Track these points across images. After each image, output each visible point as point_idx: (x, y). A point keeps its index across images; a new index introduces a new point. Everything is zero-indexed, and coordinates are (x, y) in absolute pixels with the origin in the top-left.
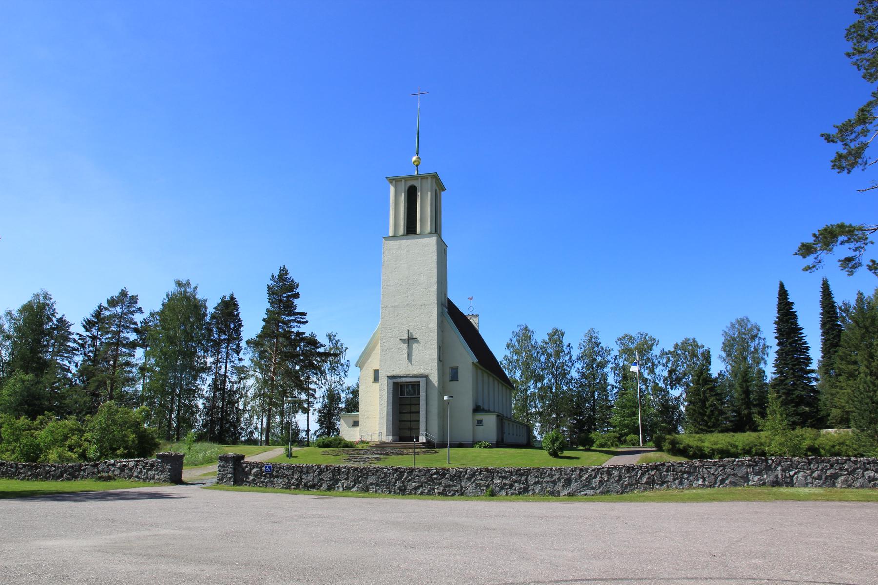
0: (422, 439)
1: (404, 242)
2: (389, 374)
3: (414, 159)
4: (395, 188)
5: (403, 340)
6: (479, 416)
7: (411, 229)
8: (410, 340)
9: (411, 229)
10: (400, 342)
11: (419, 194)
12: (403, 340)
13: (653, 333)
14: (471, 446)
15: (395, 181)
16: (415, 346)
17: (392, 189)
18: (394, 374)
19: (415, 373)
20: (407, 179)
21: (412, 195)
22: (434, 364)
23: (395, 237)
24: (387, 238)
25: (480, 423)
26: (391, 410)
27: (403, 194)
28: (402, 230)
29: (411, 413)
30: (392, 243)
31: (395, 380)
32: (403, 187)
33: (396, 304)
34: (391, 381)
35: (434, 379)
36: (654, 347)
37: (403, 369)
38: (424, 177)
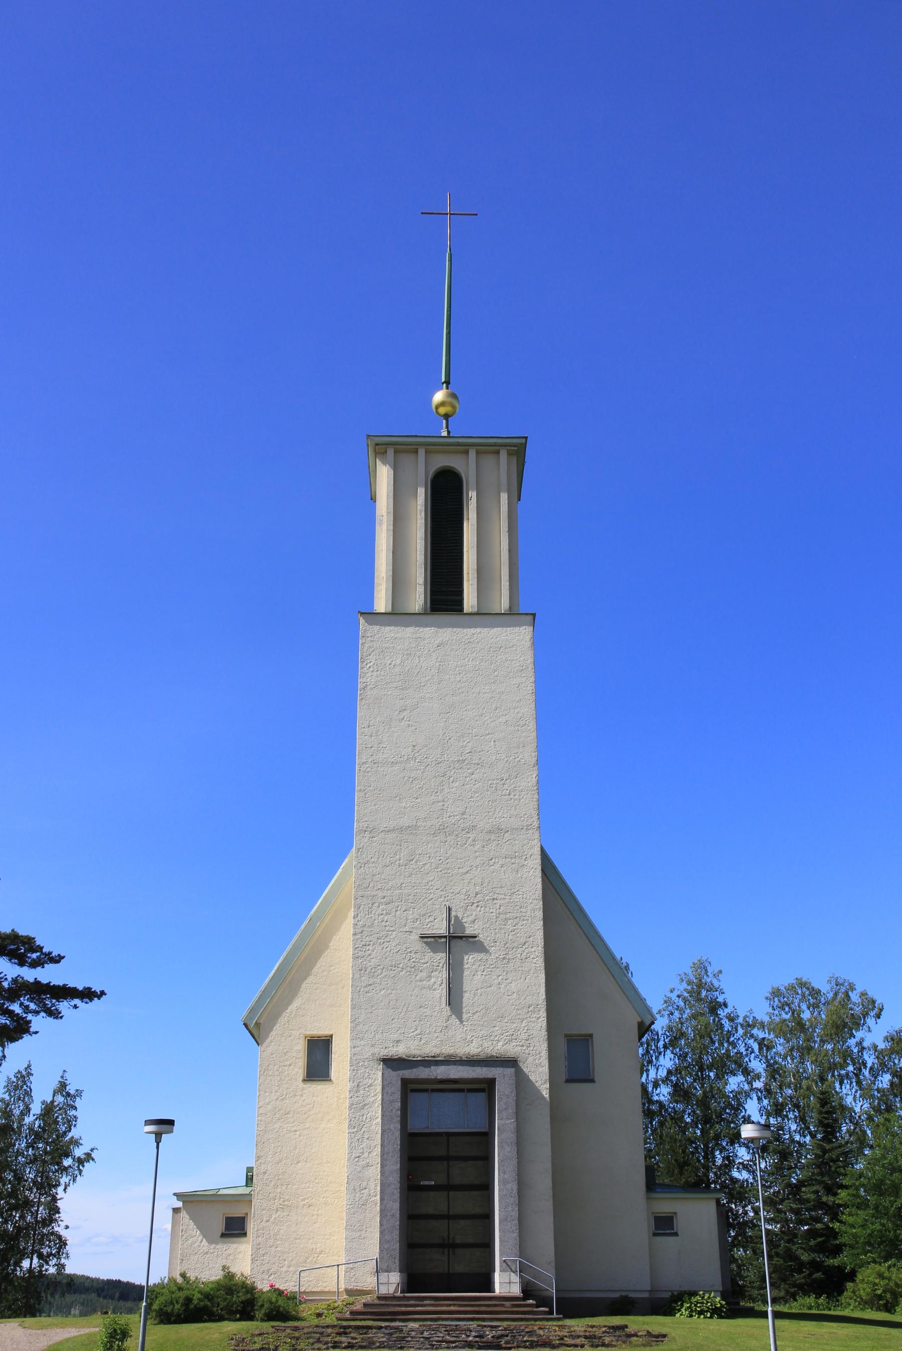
0: (505, 1283)
1: (428, 632)
2: (384, 1053)
3: (439, 396)
4: (395, 469)
5: (431, 941)
6: (665, 1205)
7: (445, 596)
8: (455, 942)
9: (445, 596)
10: (419, 945)
11: (473, 494)
12: (431, 941)
13: (867, 982)
14: (665, 1306)
15: (395, 449)
16: (471, 960)
17: (384, 475)
18: (400, 1050)
19: (473, 1049)
20: (433, 447)
21: (446, 500)
22: (538, 1023)
23: (397, 615)
24: (371, 616)
25: (664, 1225)
26: (395, 1179)
27: (421, 493)
28: (417, 597)
29: (448, 1187)
30: (389, 632)
31: (409, 1074)
32: (421, 470)
33: (405, 821)
34: (396, 1077)
35: (538, 1071)
36: (870, 1021)
37: (433, 1034)
38: (488, 448)
